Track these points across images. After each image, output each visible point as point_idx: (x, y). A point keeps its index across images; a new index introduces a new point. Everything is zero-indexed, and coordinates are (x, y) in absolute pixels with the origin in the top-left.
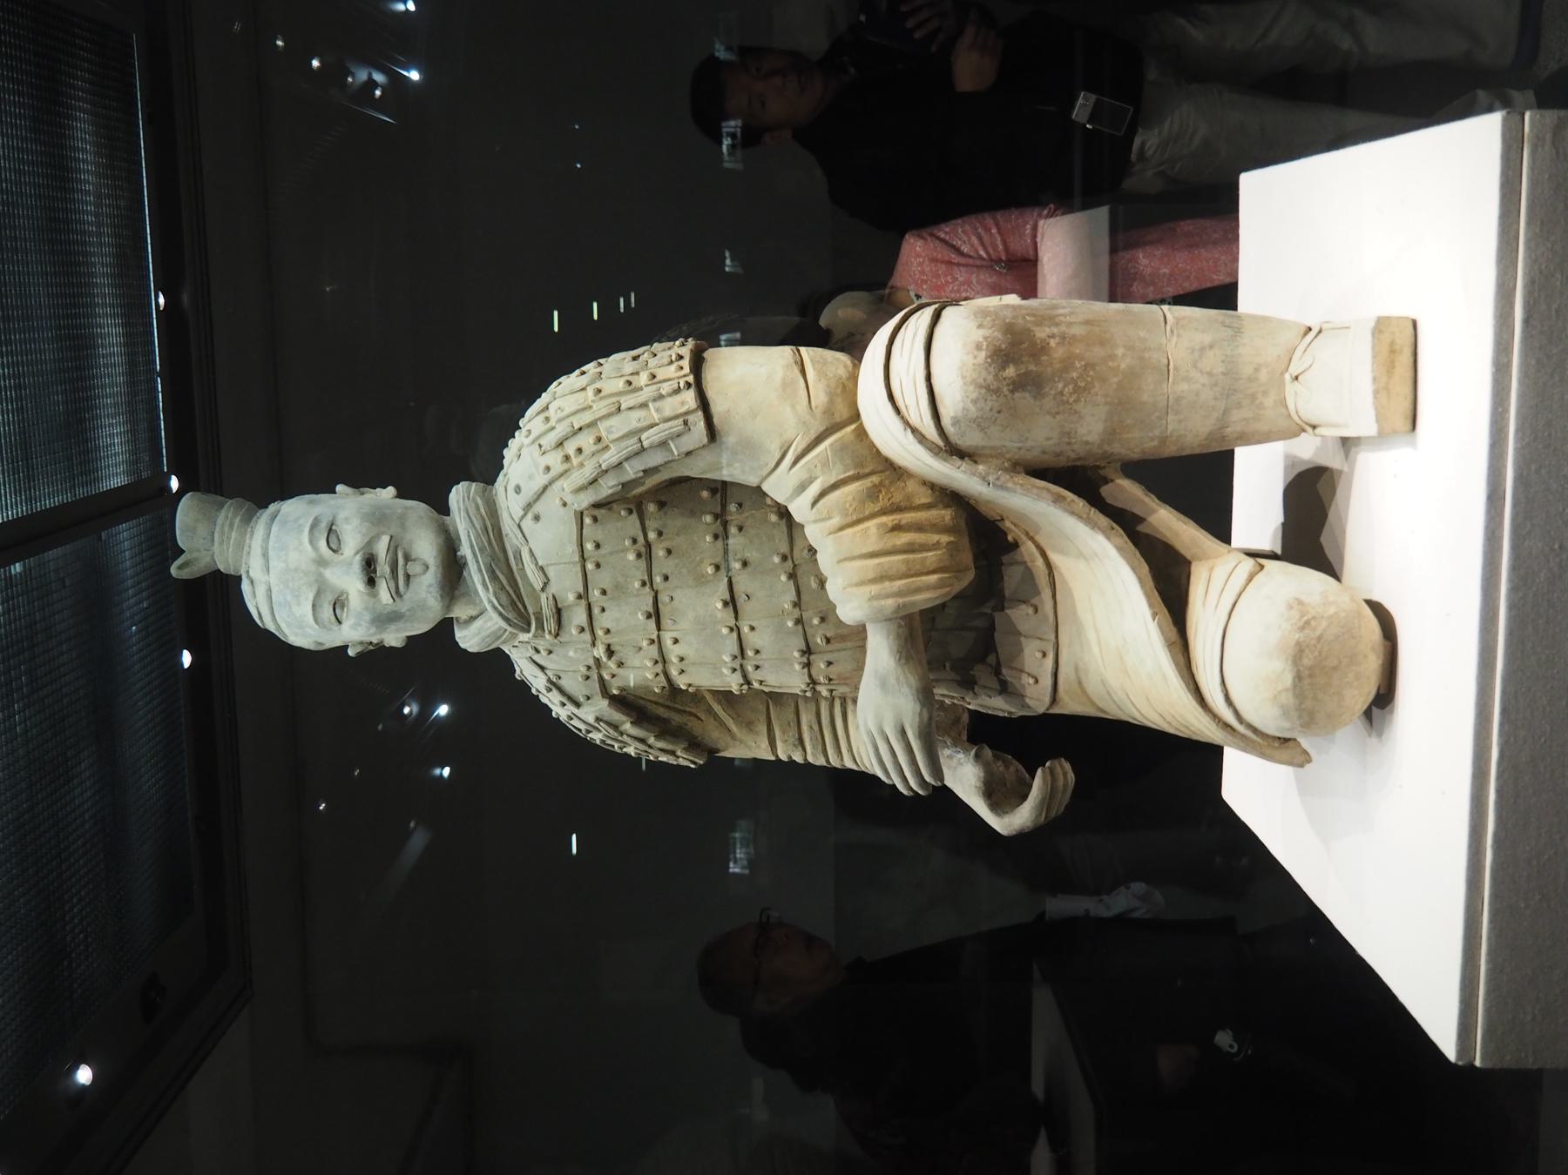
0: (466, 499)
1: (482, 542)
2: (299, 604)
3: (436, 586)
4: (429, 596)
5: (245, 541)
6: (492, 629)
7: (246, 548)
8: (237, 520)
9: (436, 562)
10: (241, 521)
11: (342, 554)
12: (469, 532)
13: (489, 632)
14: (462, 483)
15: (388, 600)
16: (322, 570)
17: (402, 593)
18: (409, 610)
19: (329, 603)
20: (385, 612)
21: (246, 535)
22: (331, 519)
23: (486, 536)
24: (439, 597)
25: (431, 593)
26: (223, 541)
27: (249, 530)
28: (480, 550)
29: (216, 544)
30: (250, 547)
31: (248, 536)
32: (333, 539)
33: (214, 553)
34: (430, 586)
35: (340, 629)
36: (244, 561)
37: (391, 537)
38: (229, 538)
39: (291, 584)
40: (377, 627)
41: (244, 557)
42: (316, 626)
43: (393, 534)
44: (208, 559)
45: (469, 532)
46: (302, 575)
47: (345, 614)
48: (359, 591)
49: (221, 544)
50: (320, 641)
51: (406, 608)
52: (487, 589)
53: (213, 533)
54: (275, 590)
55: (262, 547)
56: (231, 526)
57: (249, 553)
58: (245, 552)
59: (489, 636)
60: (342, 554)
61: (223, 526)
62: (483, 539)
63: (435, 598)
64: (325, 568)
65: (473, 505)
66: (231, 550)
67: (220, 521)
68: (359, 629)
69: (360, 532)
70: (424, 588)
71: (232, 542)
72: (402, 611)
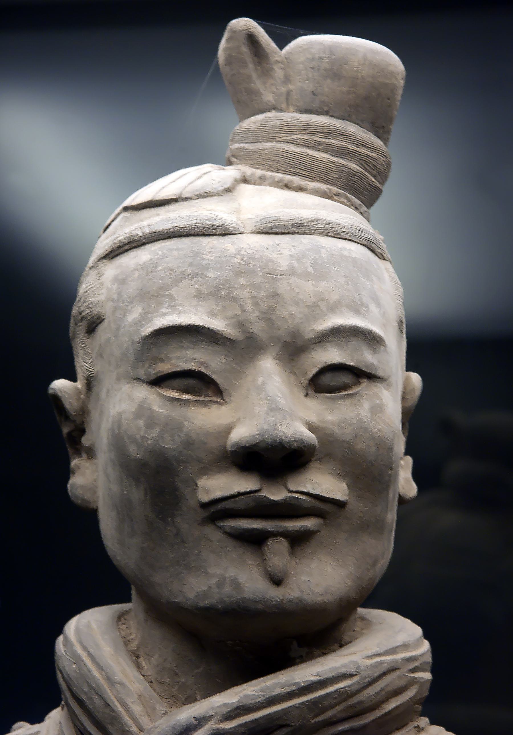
0: (412, 666)
1: (332, 707)
2: (199, 296)
3: (237, 596)
4: (213, 581)
5: (312, 179)
6: (125, 717)
7: (297, 180)
8: (354, 166)
9: (290, 601)
10: (352, 173)
11: (307, 395)
12: (352, 675)
13: (119, 708)
14: (426, 645)
15: (207, 491)
16: (275, 350)
17: (221, 524)
18: (177, 534)
19: (202, 363)
20: (179, 484)
21: (325, 182)
22: (380, 374)
23: (343, 715)
24: (207, 602)
25: (220, 585)
26: (312, 133)
27: (335, 189)
28: (315, 702)
29: (304, 118)
30: (300, 189)
31: (324, 187)
32: (345, 378)
33: (281, 110)
34: (236, 585)
35: (137, 379)
36: (269, 174)
37: (340, 505)
38: (317, 146)
39: (243, 281)
40: (142, 465)
41: (279, 176)
42: (148, 330)
43: (349, 507)
44: (269, 97)
45: (352, 675)
46: (264, 306)
47: (175, 395)
48: (229, 429)
49: (305, 129)
50: (101, 328)
51: (184, 527)
52: (229, 717)
53: (326, 113)
54: (225, 243)
55: (316, 221)
56: (343, 153)
57: (287, 186)
58: (288, 177)
59: (107, 705)
60: (307, 395)
61: (344, 135)
62: (339, 708)
63: (205, 595)
64: (278, 357)
65: (402, 683)
66: (292, 148)
67: (352, 128)
68: (141, 423)
69: (356, 437)
70: (232, 572)
71: (311, 152)
72: (178, 520)
